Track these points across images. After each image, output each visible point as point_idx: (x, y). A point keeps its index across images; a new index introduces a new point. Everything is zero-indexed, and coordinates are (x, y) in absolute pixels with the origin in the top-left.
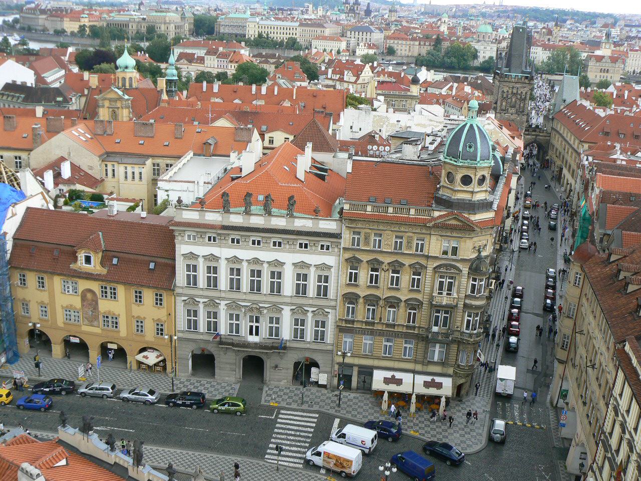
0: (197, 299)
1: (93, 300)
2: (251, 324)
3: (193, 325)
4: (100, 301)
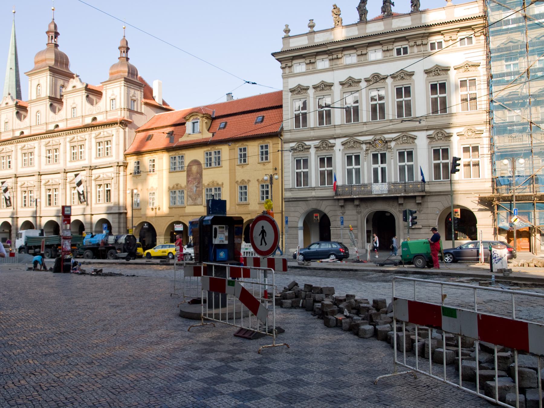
0: (307, 143)
1: (197, 173)
2: (376, 166)
3: (302, 179)
4: (205, 172)
